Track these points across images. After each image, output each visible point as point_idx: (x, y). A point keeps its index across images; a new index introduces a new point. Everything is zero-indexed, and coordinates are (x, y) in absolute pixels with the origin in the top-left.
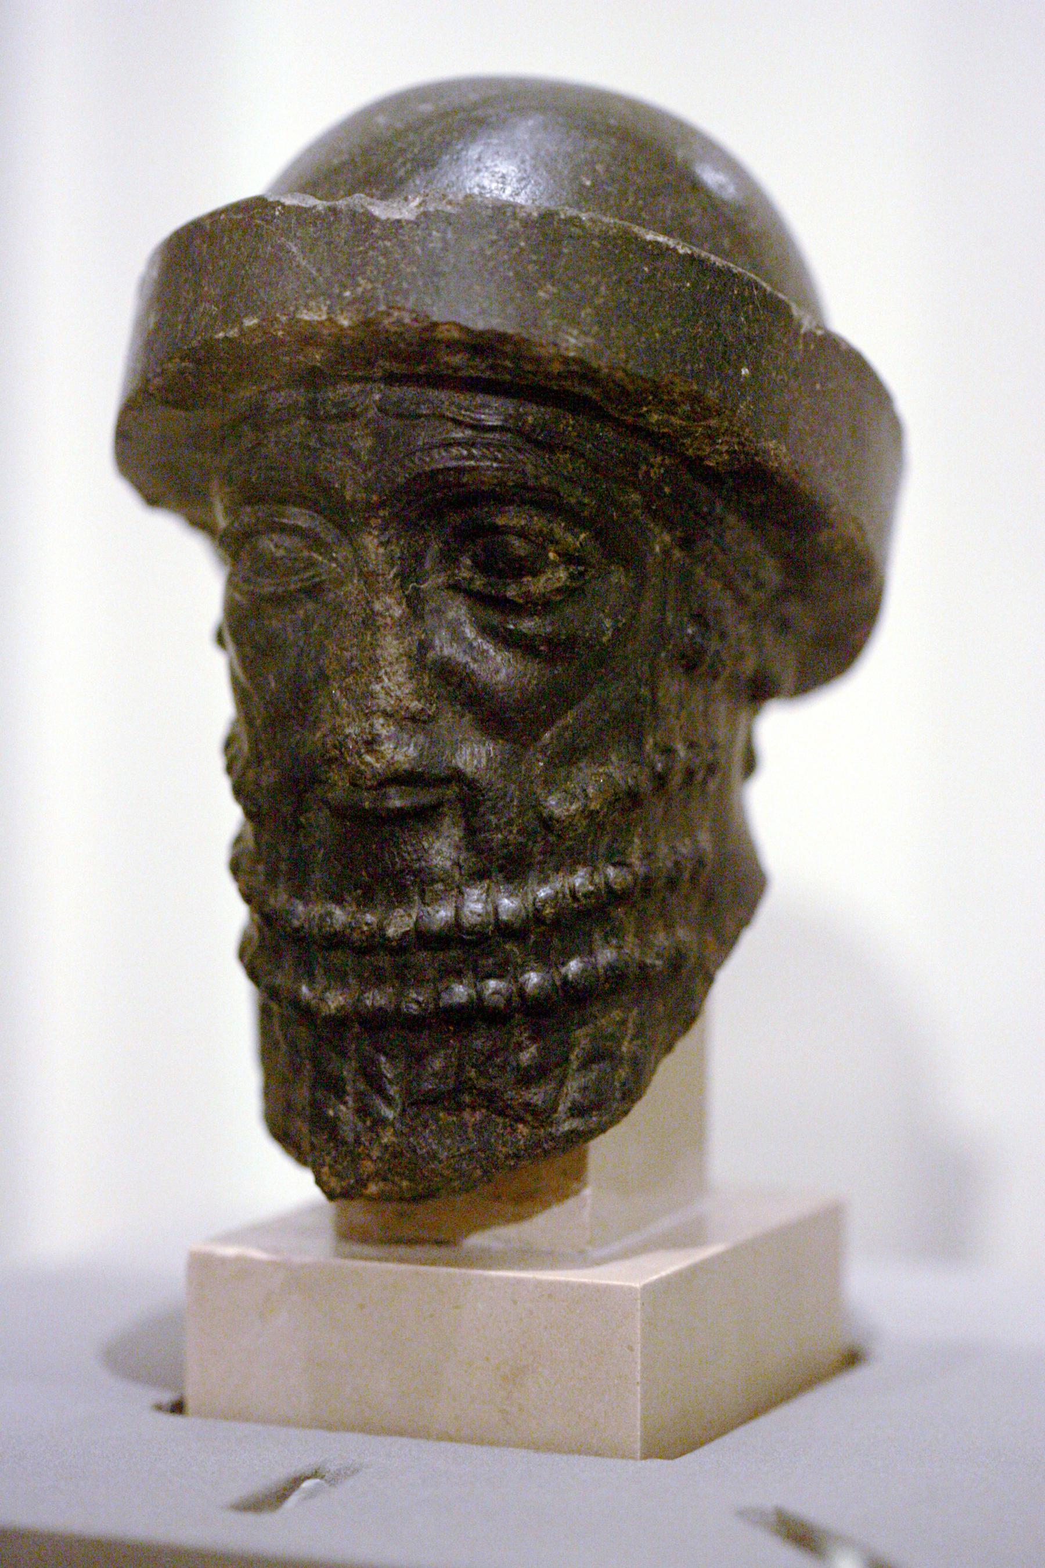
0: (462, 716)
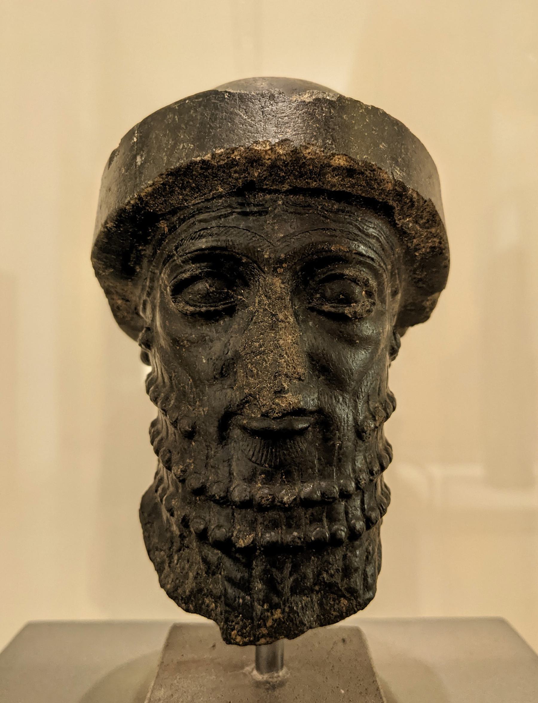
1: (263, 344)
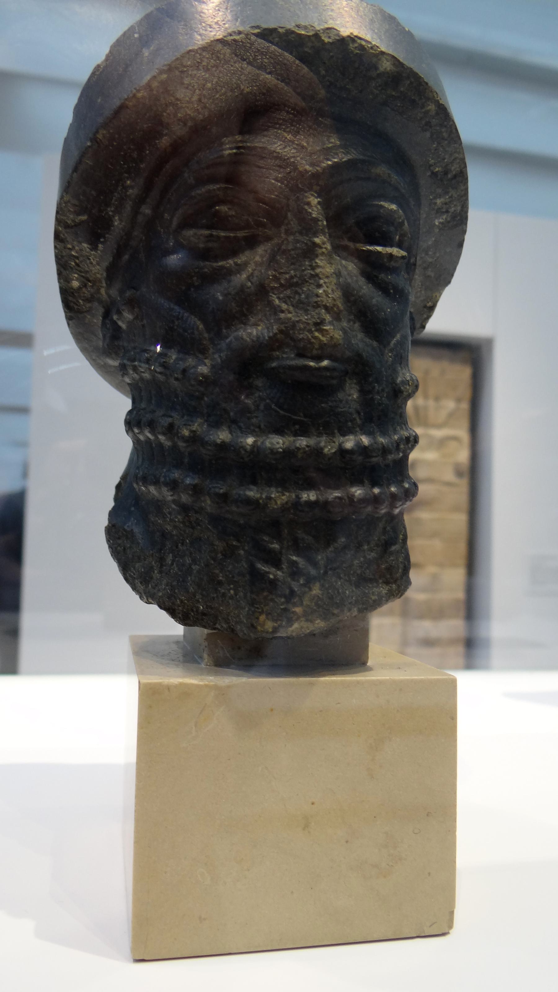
0: (354, 323)
1: (295, 276)
